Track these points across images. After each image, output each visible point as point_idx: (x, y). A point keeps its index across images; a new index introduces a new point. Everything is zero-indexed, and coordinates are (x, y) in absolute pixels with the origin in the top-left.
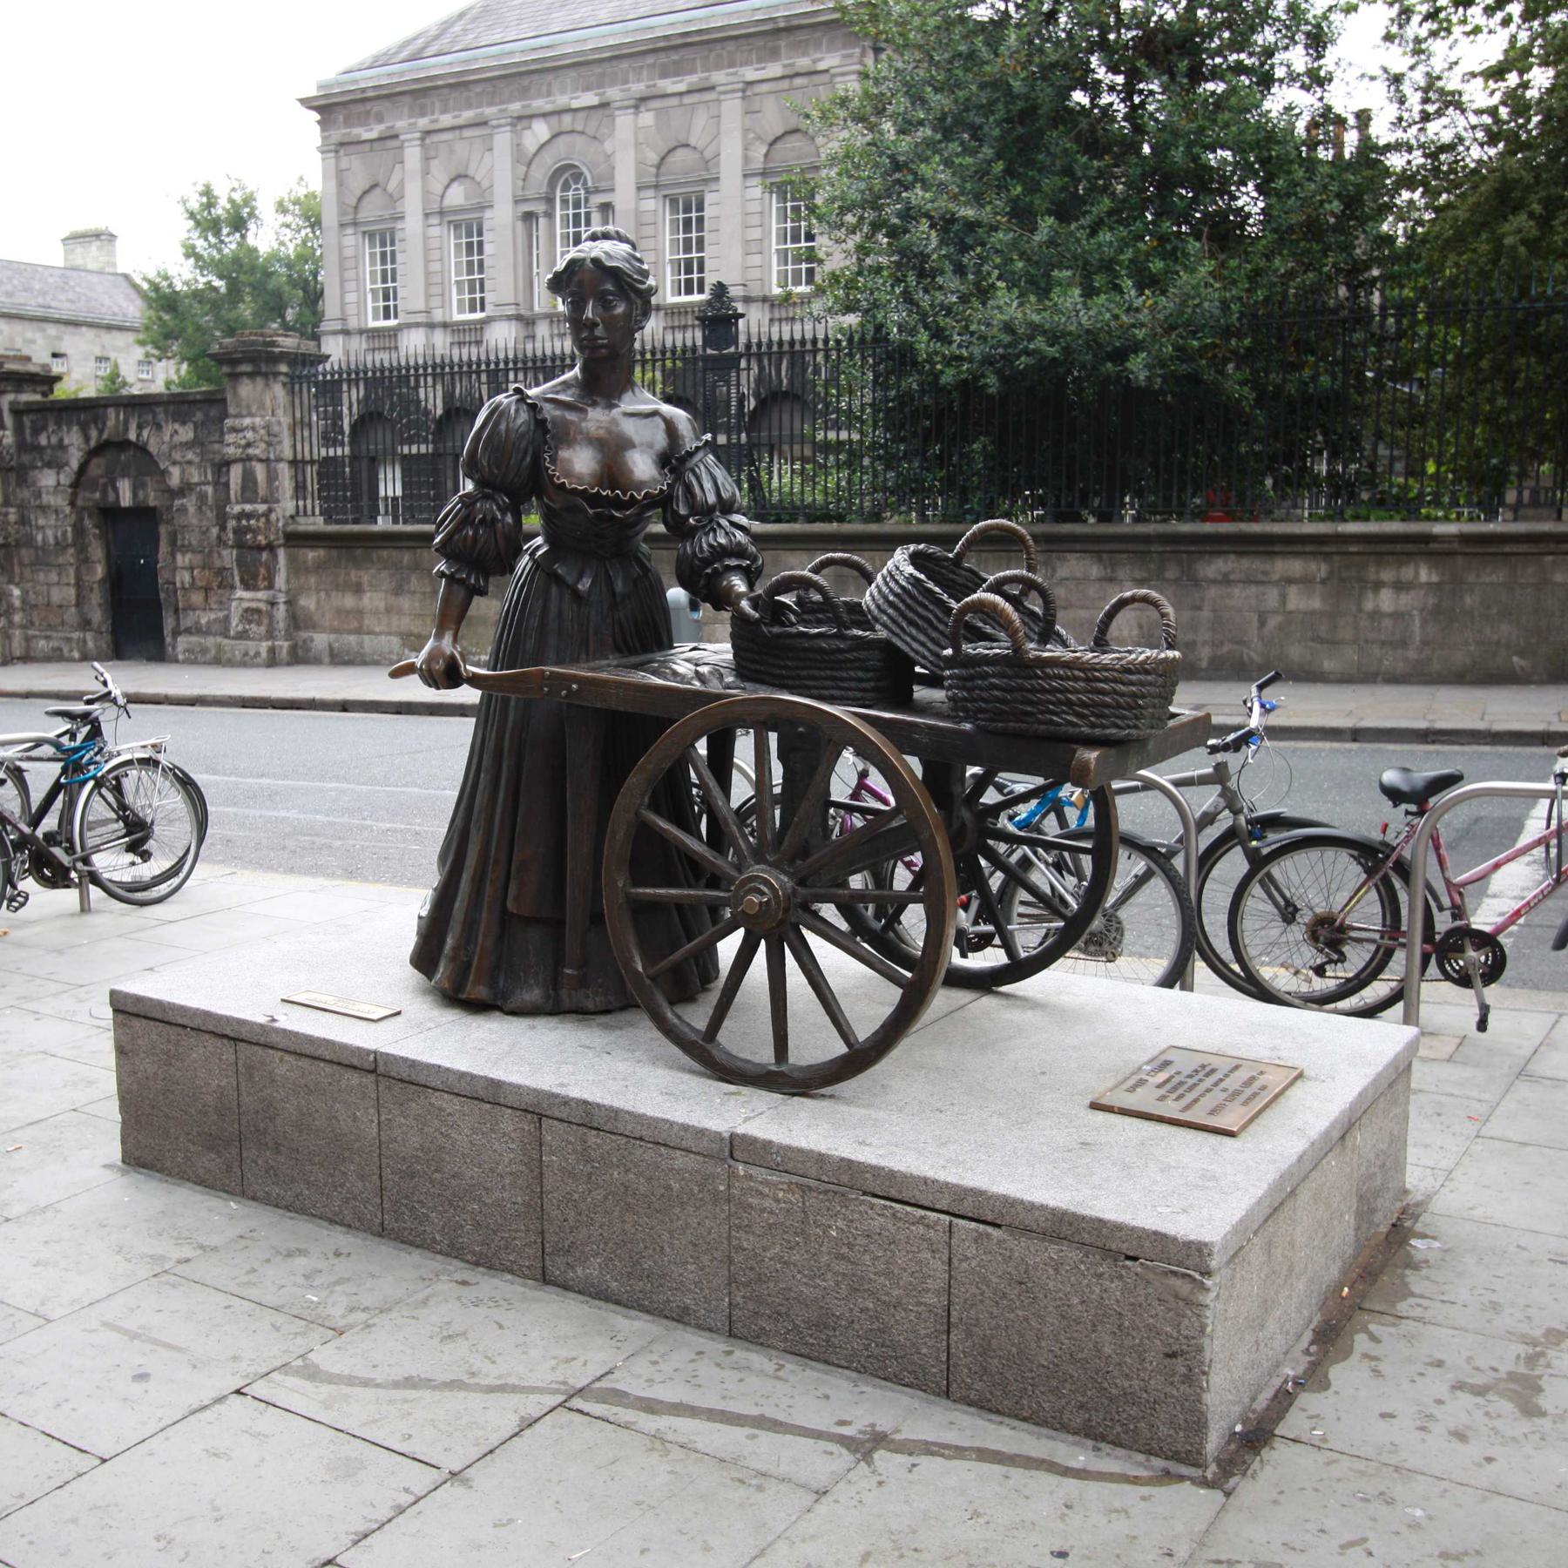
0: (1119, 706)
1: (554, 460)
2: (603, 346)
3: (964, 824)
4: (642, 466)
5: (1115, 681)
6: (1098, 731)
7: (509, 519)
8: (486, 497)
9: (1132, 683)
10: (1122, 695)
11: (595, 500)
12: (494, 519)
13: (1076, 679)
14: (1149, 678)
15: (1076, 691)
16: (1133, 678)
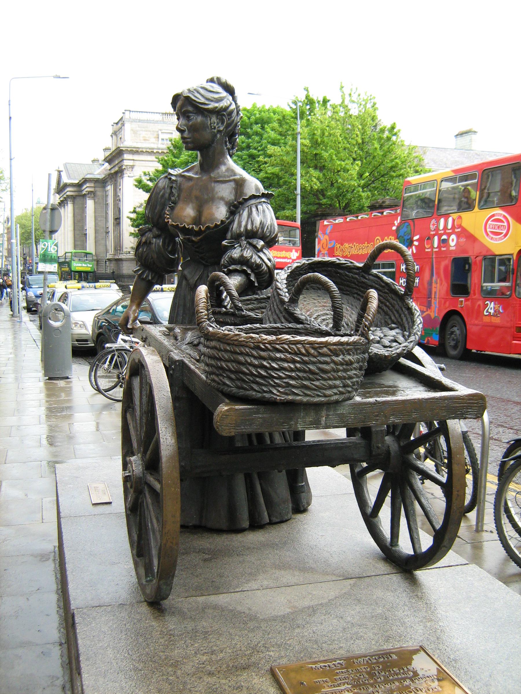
0: (252, 374)
1: (172, 208)
2: (190, 143)
3: (388, 452)
4: (220, 212)
5: (248, 355)
6: (242, 392)
7: (160, 242)
8: (150, 230)
9: (264, 359)
10: (255, 366)
11: (185, 231)
12: (150, 243)
13: (226, 351)
14: (278, 355)
15: (226, 361)
16: (262, 353)
